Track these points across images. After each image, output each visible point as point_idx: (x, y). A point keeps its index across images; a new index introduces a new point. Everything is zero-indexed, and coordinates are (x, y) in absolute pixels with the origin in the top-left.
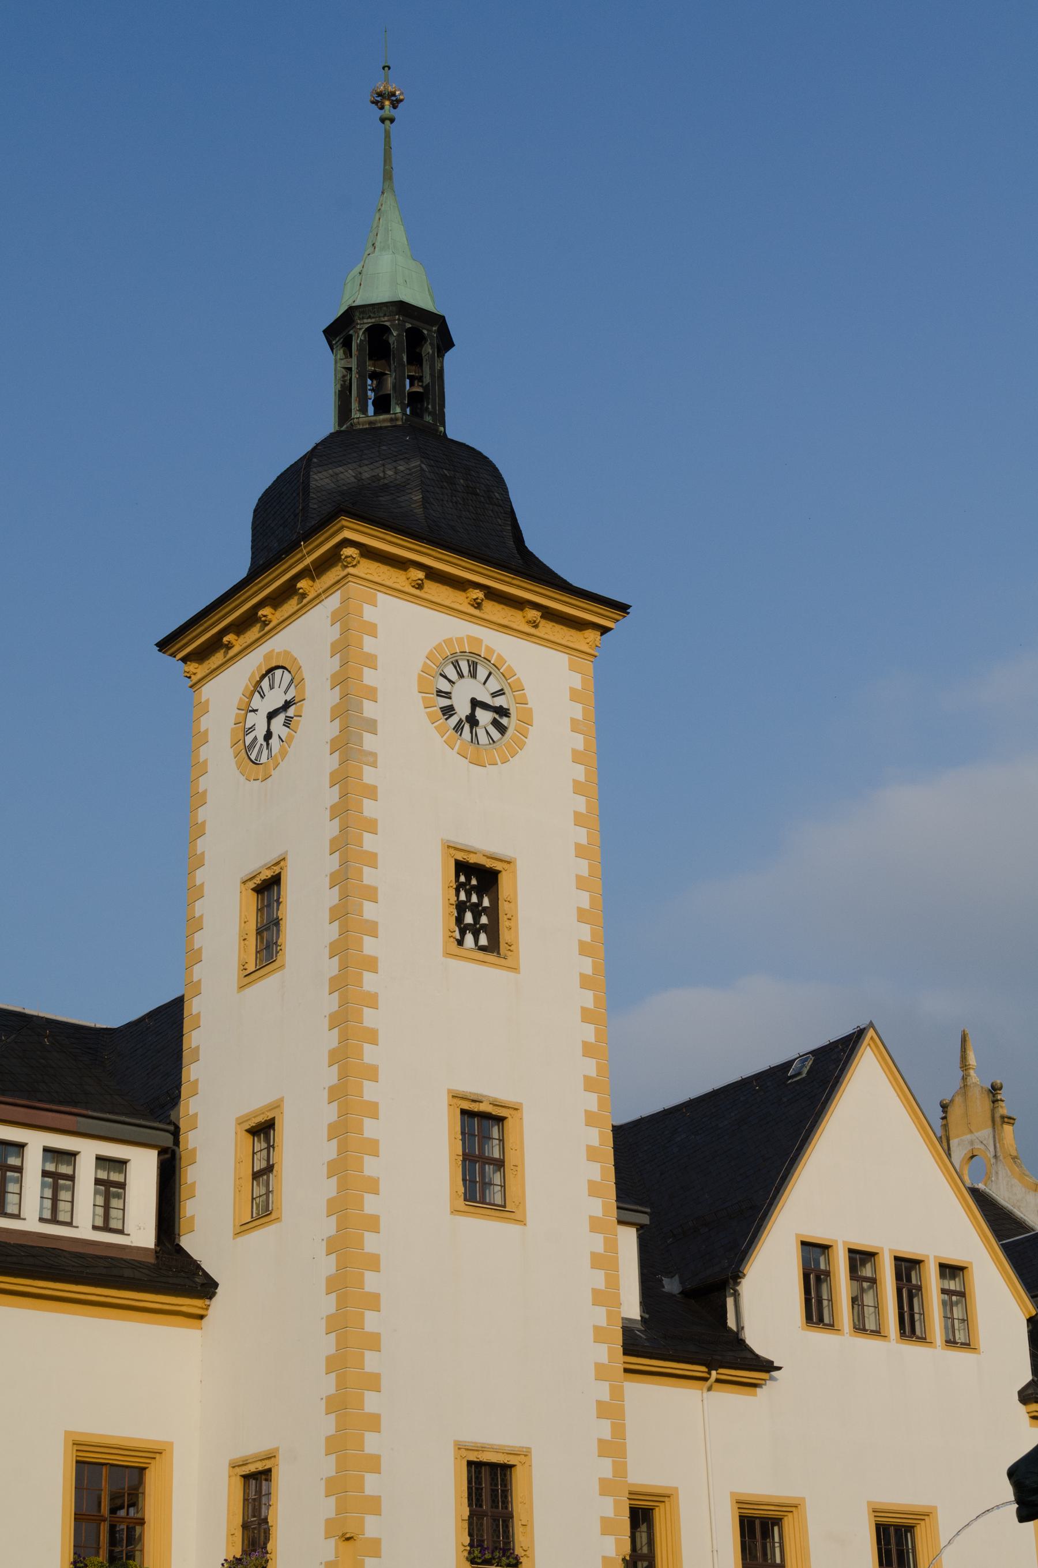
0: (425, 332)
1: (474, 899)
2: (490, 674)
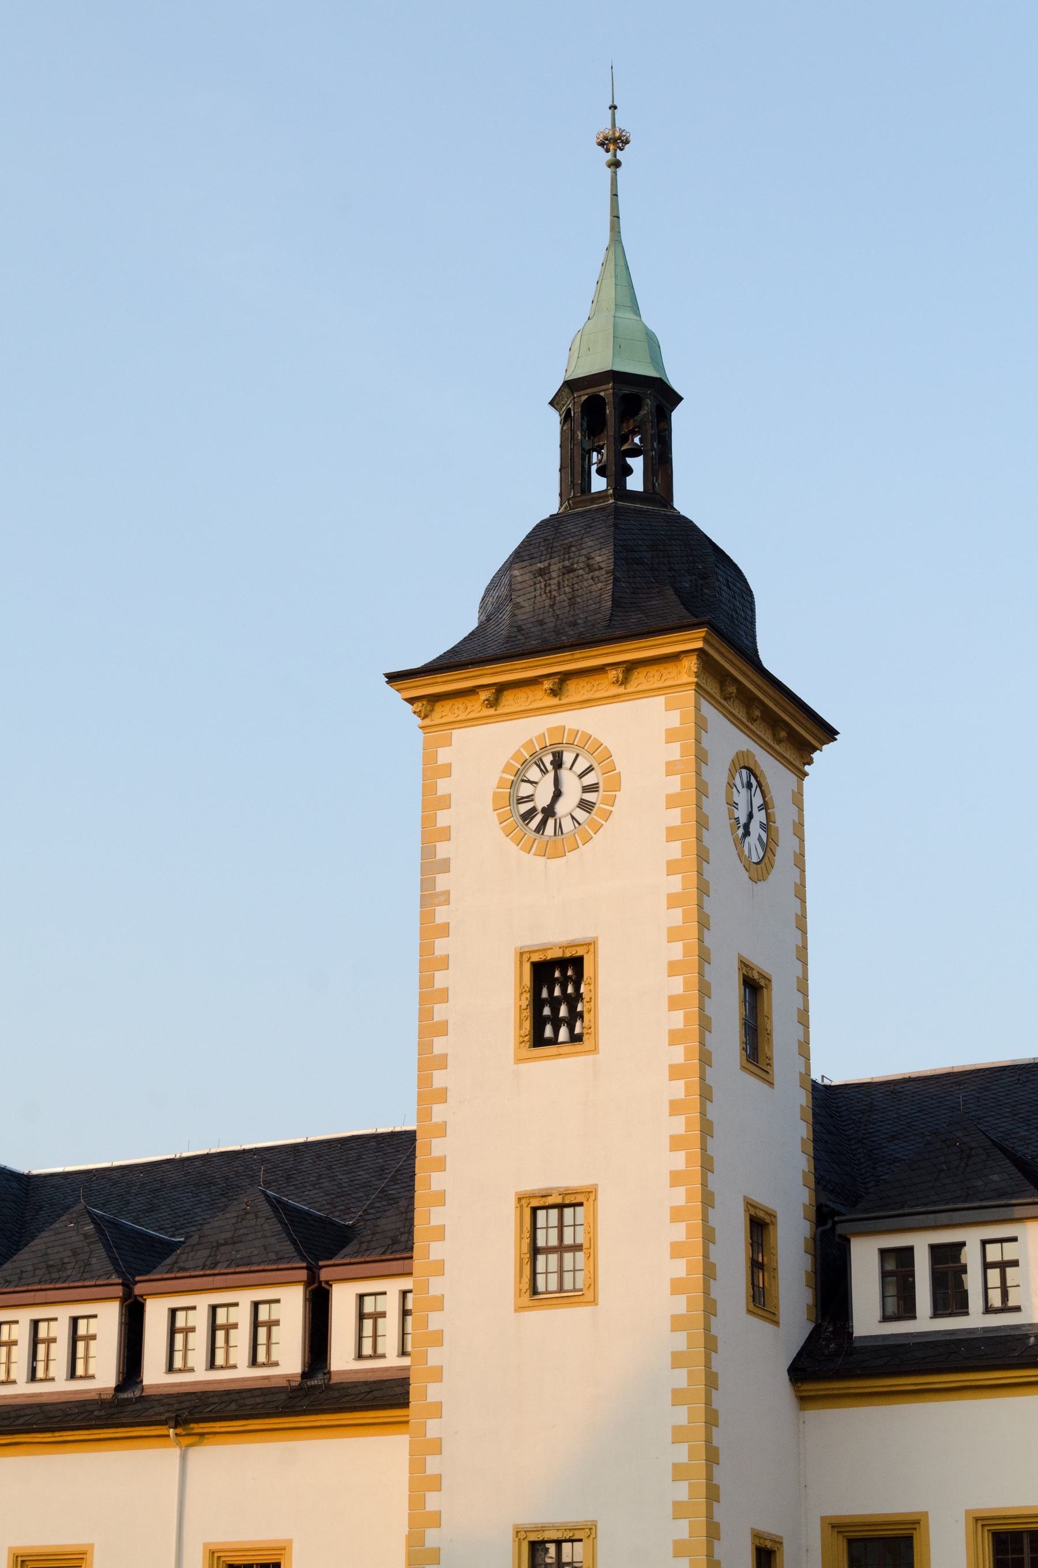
0: (602, 394)
2: (577, 755)
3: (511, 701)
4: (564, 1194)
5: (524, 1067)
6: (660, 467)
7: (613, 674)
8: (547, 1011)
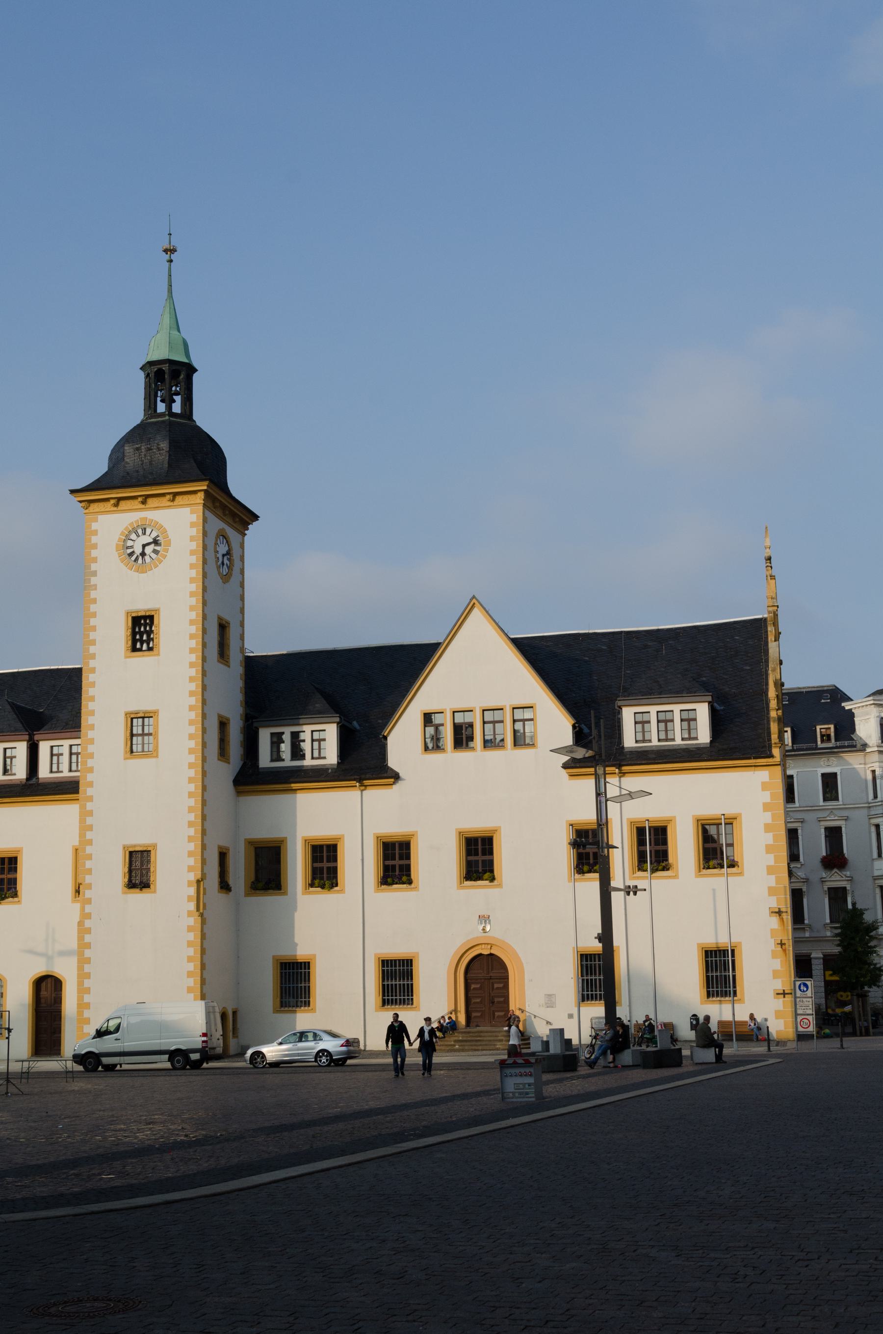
3: (123, 505)
4: (145, 712)
5: (128, 660)
6: (188, 401)
7: (168, 497)
8: (138, 637)
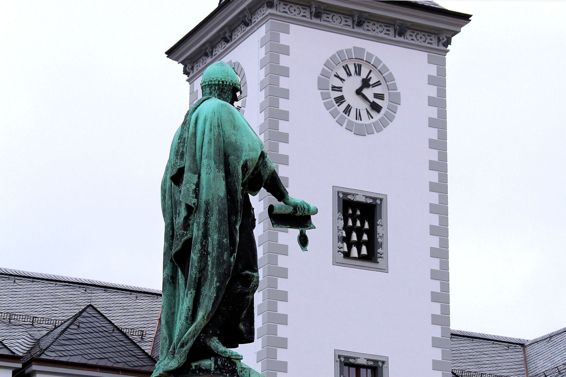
1: (358, 224)
2: (371, 71)
